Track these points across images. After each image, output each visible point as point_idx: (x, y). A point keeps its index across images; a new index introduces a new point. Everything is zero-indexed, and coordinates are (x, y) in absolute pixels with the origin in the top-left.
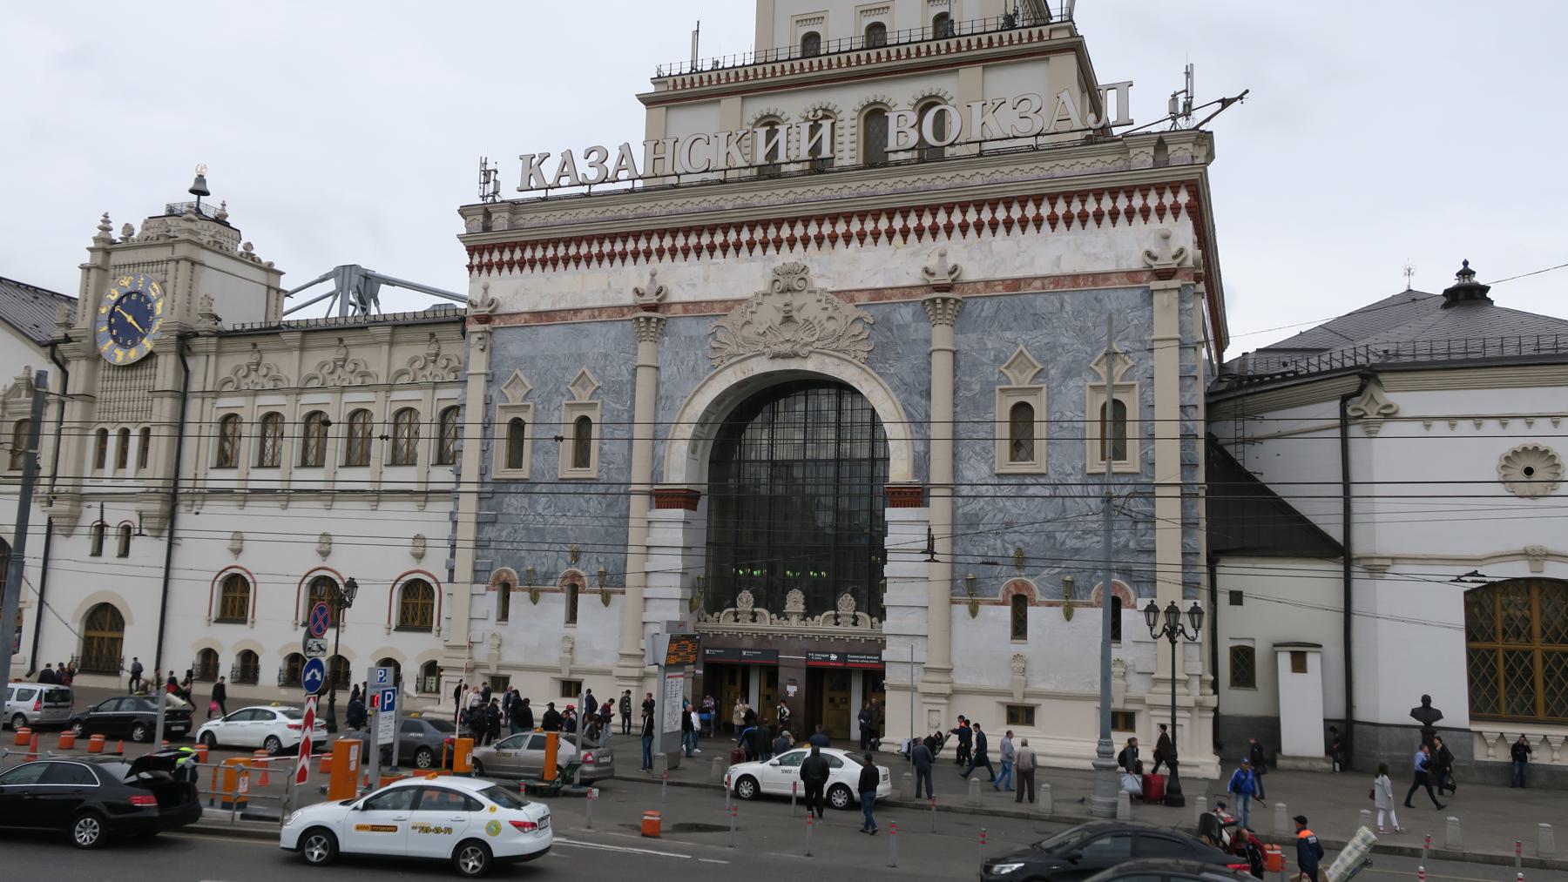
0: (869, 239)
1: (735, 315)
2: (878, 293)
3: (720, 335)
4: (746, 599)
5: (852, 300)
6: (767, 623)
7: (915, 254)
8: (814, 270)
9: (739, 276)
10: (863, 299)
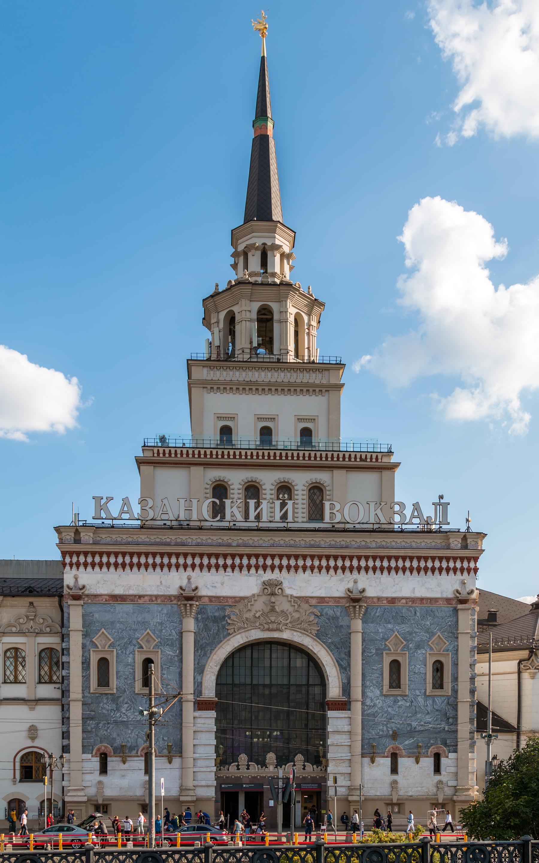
0: (316, 570)
1: (241, 606)
2: (321, 599)
3: (233, 617)
4: (243, 758)
5: (307, 602)
6: (255, 770)
7: (341, 580)
8: (285, 585)
9: (243, 584)
10: (314, 602)
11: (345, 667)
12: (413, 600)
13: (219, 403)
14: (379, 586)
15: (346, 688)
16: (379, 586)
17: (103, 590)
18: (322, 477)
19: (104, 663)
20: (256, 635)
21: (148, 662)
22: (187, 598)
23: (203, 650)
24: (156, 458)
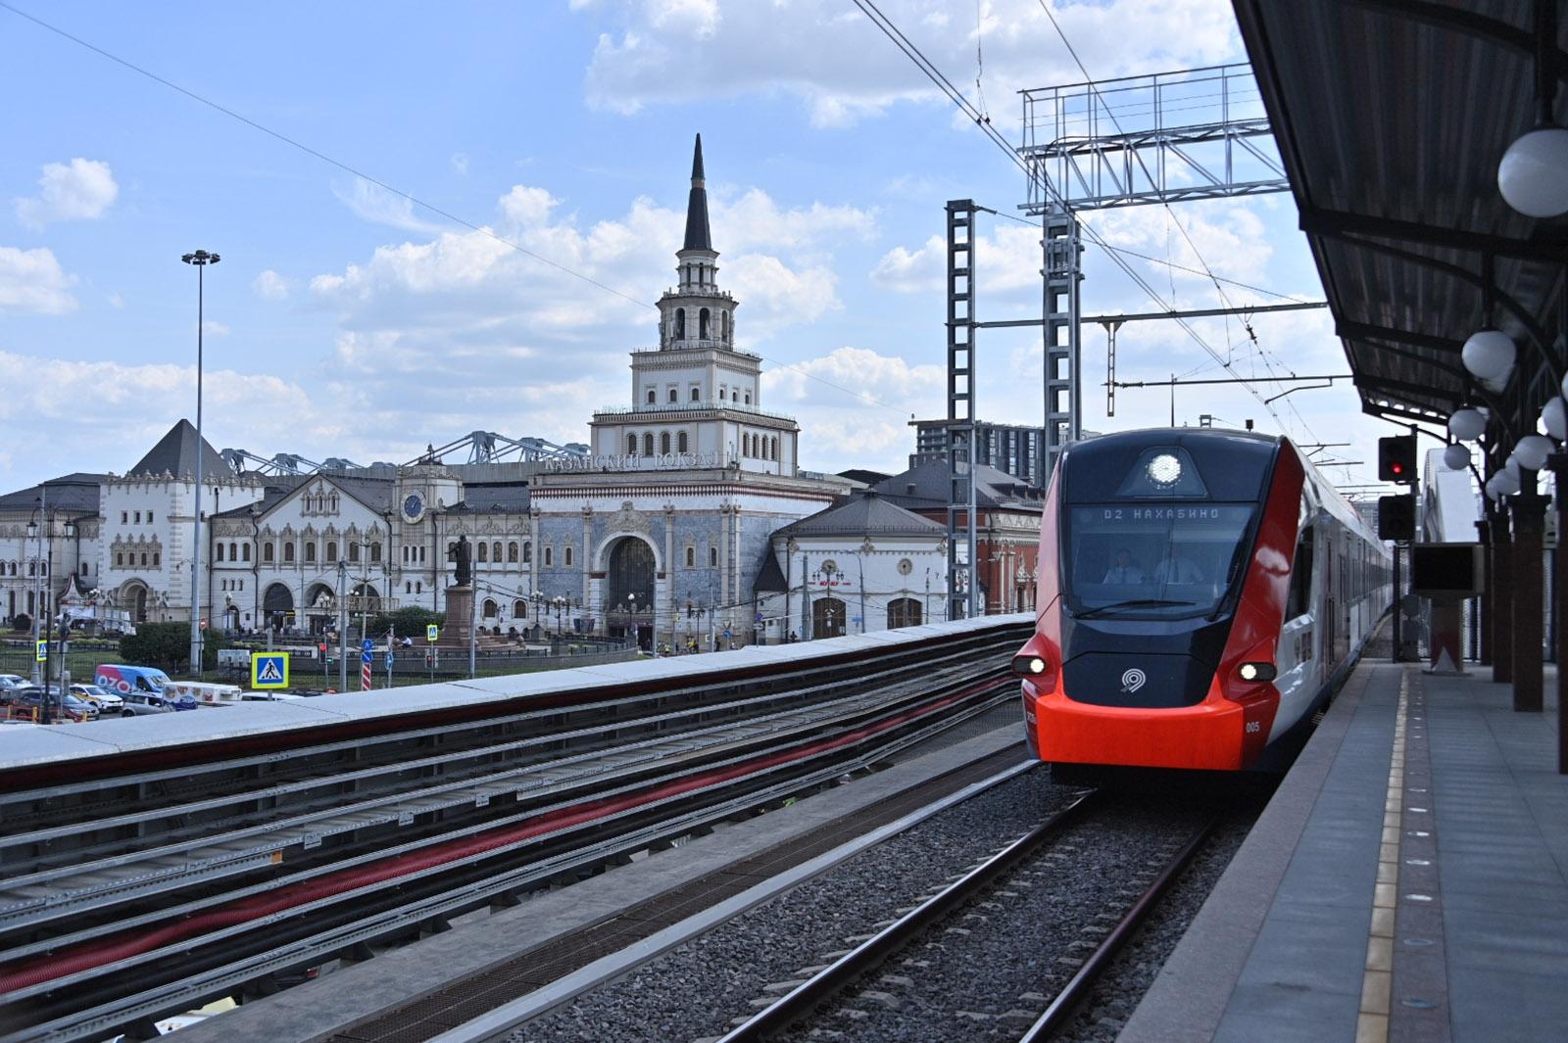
2: (652, 512)
11: (663, 553)
12: (699, 511)
13: (648, 377)
14: (681, 503)
15: (664, 565)
16: (681, 503)
17: (547, 511)
18: (686, 427)
19: (548, 550)
20: (620, 534)
21: (569, 550)
22: (588, 513)
23: (594, 542)
24: (601, 422)
